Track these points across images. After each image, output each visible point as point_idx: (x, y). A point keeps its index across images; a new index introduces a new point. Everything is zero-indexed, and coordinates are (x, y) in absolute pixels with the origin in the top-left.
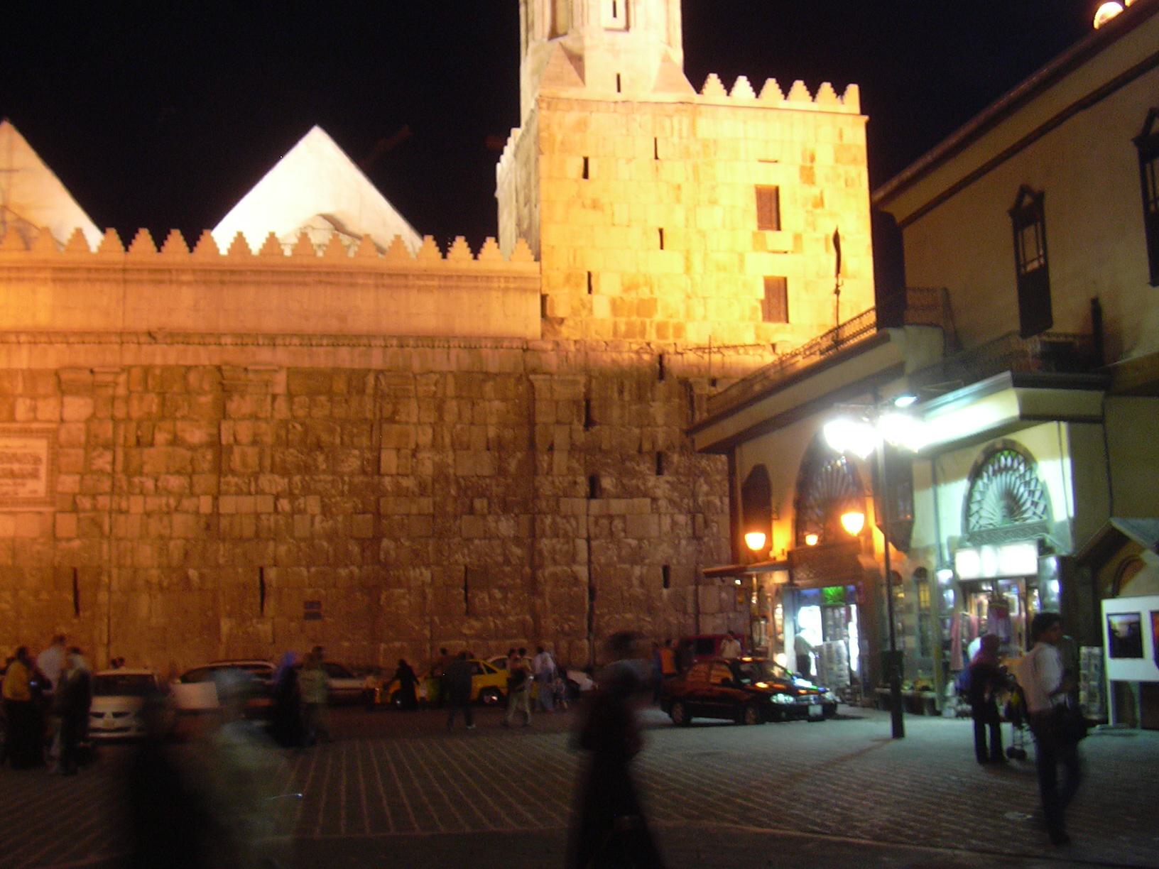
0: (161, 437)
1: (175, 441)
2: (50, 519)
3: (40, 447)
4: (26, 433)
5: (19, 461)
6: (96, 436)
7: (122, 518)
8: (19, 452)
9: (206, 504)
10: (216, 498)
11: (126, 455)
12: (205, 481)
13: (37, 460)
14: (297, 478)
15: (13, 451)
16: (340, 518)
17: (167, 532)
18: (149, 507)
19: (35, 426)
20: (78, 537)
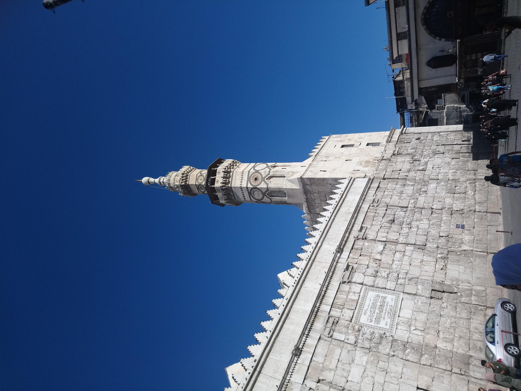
0: (378, 257)
1: (381, 253)
2: (406, 295)
3: (372, 294)
4: (364, 297)
5: (376, 302)
6: (372, 274)
7: (410, 272)
8: (372, 301)
9: (411, 248)
10: (408, 244)
11: (383, 268)
12: (400, 247)
13: (378, 296)
14: (404, 226)
15: (371, 304)
16: (422, 217)
17: (420, 261)
18: (408, 263)
19: (362, 294)
20: (417, 286)
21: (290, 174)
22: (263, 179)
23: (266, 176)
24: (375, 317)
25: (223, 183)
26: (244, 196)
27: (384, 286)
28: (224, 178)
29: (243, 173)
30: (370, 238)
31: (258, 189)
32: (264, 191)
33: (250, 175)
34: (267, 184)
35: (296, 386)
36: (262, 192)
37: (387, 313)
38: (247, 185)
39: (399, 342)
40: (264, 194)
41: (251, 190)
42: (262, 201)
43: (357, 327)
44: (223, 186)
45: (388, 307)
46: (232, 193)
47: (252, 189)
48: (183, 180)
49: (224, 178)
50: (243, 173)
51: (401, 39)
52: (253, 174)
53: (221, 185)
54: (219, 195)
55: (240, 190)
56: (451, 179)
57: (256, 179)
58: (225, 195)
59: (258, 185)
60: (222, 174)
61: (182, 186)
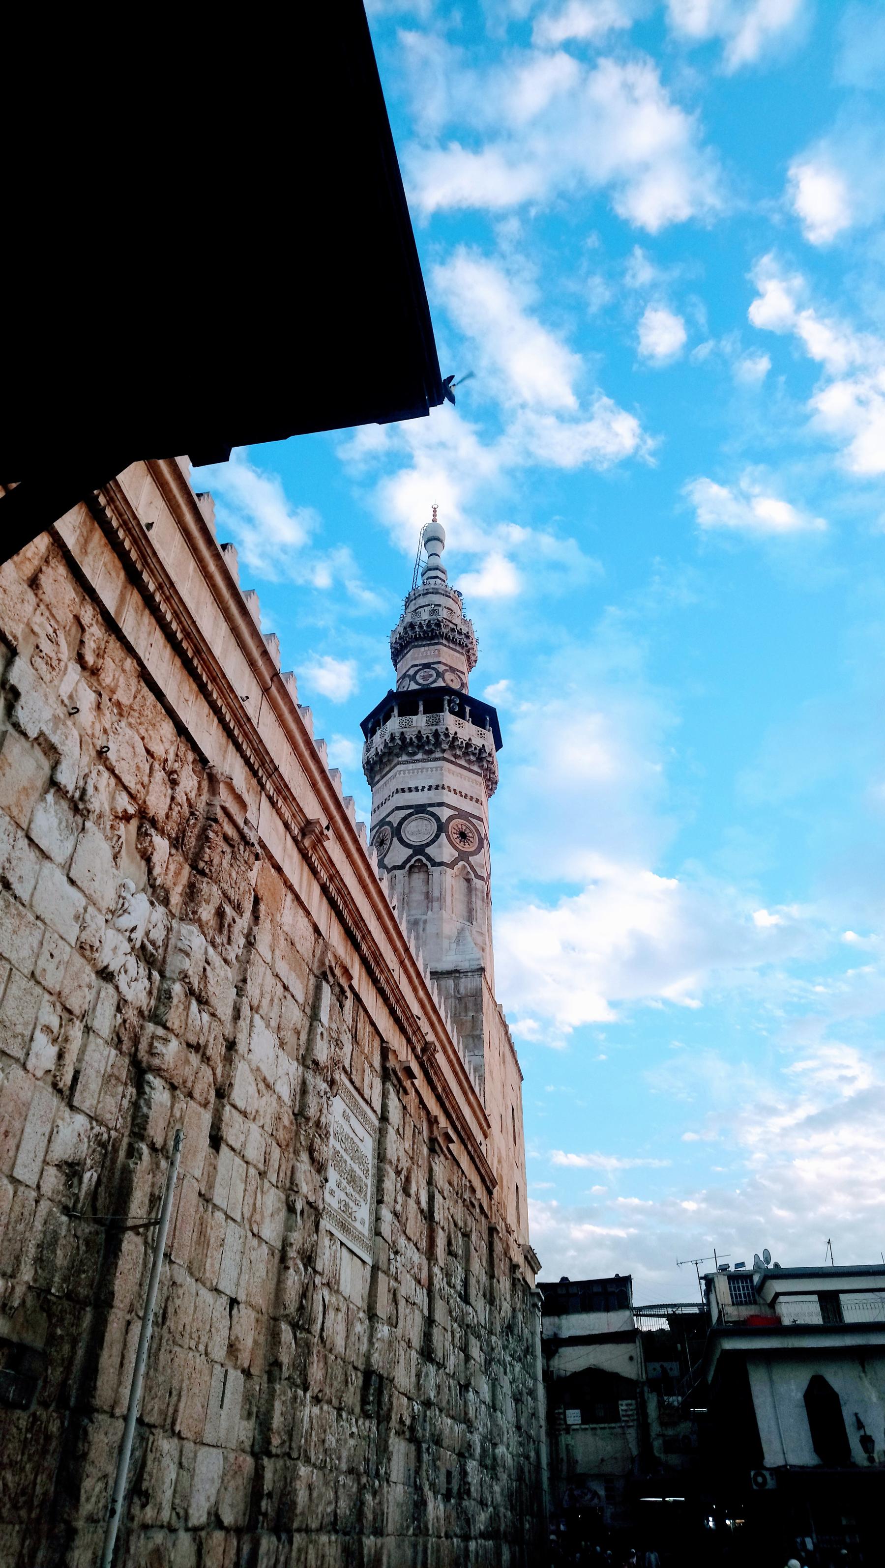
21: (479, 939)
22: (464, 856)
23: (472, 867)
24: (342, 1152)
25: (455, 738)
26: (410, 790)
27: (385, 1198)
28: (468, 745)
29: (477, 801)
30: (433, 1164)
31: (437, 836)
32: (428, 850)
33: (474, 821)
34: (451, 865)
36: (428, 845)
37: (347, 1200)
38: (449, 806)
39: (315, 1235)
40: (419, 850)
41: (433, 815)
42: (395, 839)
43: (337, 1077)
44: (447, 735)
45: (355, 1208)
46: (419, 756)
47: (438, 819)
48: (453, 630)
49: (468, 745)
50: (477, 801)
51: (820, 1300)
52: (477, 831)
53: (452, 732)
54: (420, 721)
55: (433, 783)
56: (497, 1451)
57: (463, 835)
58: (419, 736)
59: (448, 837)
60: (477, 742)
61: (438, 624)
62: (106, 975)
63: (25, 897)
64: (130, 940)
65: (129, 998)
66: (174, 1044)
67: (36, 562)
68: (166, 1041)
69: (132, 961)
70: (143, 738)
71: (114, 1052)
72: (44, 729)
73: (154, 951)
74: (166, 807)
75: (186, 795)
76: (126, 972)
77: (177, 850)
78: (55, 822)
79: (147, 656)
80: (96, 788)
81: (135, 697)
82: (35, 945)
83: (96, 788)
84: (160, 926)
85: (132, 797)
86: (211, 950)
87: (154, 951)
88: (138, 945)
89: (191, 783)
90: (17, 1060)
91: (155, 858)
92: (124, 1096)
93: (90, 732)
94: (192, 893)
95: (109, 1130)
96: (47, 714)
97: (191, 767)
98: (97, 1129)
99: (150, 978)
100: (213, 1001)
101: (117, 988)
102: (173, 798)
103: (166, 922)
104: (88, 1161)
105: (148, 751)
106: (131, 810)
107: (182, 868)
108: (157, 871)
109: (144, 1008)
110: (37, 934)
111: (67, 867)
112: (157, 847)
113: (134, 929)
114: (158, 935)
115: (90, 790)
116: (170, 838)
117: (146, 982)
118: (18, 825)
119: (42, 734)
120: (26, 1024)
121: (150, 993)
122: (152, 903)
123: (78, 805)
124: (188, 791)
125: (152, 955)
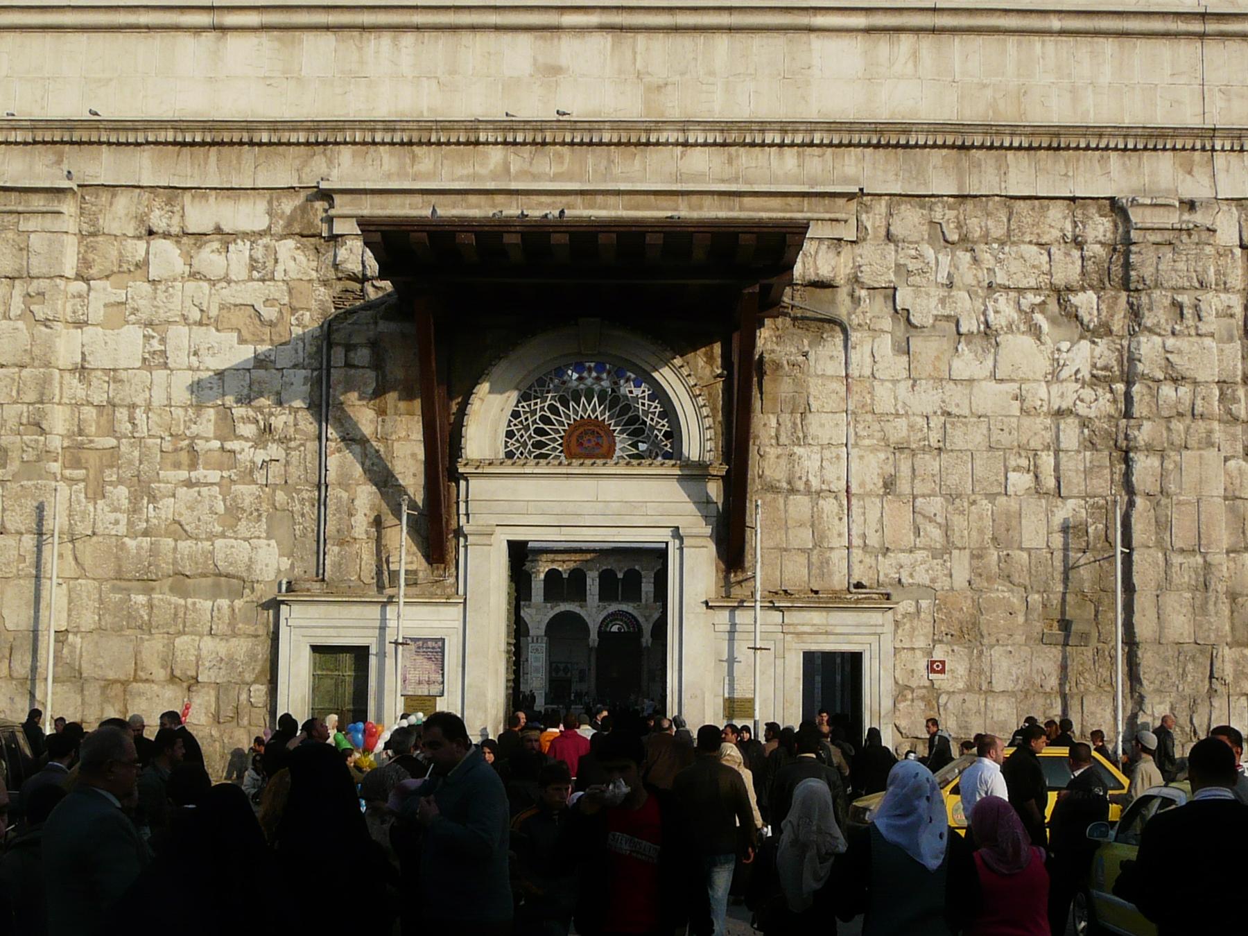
35: (1206, 181)
62: (1060, 413)
63: (966, 412)
64: (1077, 380)
65: (1092, 415)
66: (1147, 425)
67: (884, 223)
68: (1139, 427)
69: (1087, 393)
70: (1030, 242)
71: (1088, 453)
72: (935, 313)
73: (1108, 373)
74: (1078, 270)
75: (1100, 242)
76: (1082, 401)
77: (1103, 289)
78: (972, 356)
79: (1003, 185)
80: (997, 312)
81: (1009, 220)
82: (985, 432)
83: (997, 312)
84: (1106, 353)
85: (1037, 290)
86: (1171, 342)
87: (1108, 373)
88: (1088, 377)
89: (1101, 229)
90: (999, 494)
91: (1081, 312)
92: (1112, 473)
93: (974, 283)
94: (1135, 313)
95: (1104, 498)
96: (934, 302)
97: (1096, 217)
98: (1091, 501)
99: (1111, 391)
100: (1187, 374)
101: (1077, 415)
102: (1083, 258)
103: (1113, 346)
104: (1090, 520)
105: (1039, 244)
106: (1038, 300)
107: (1116, 298)
108: (1086, 320)
109: (1113, 412)
110: (984, 427)
111: (993, 376)
112: (1079, 304)
113: (1078, 371)
114: (1111, 359)
115: (991, 316)
116: (1092, 287)
117: (1109, 396)
118: (941, 380)
119: (936, 318)
120: (997, 474)
121: (1115, 401)
122: (1094, 342)
123: (988, 332)
124: (1101, 238)
125: (1105, 377)
